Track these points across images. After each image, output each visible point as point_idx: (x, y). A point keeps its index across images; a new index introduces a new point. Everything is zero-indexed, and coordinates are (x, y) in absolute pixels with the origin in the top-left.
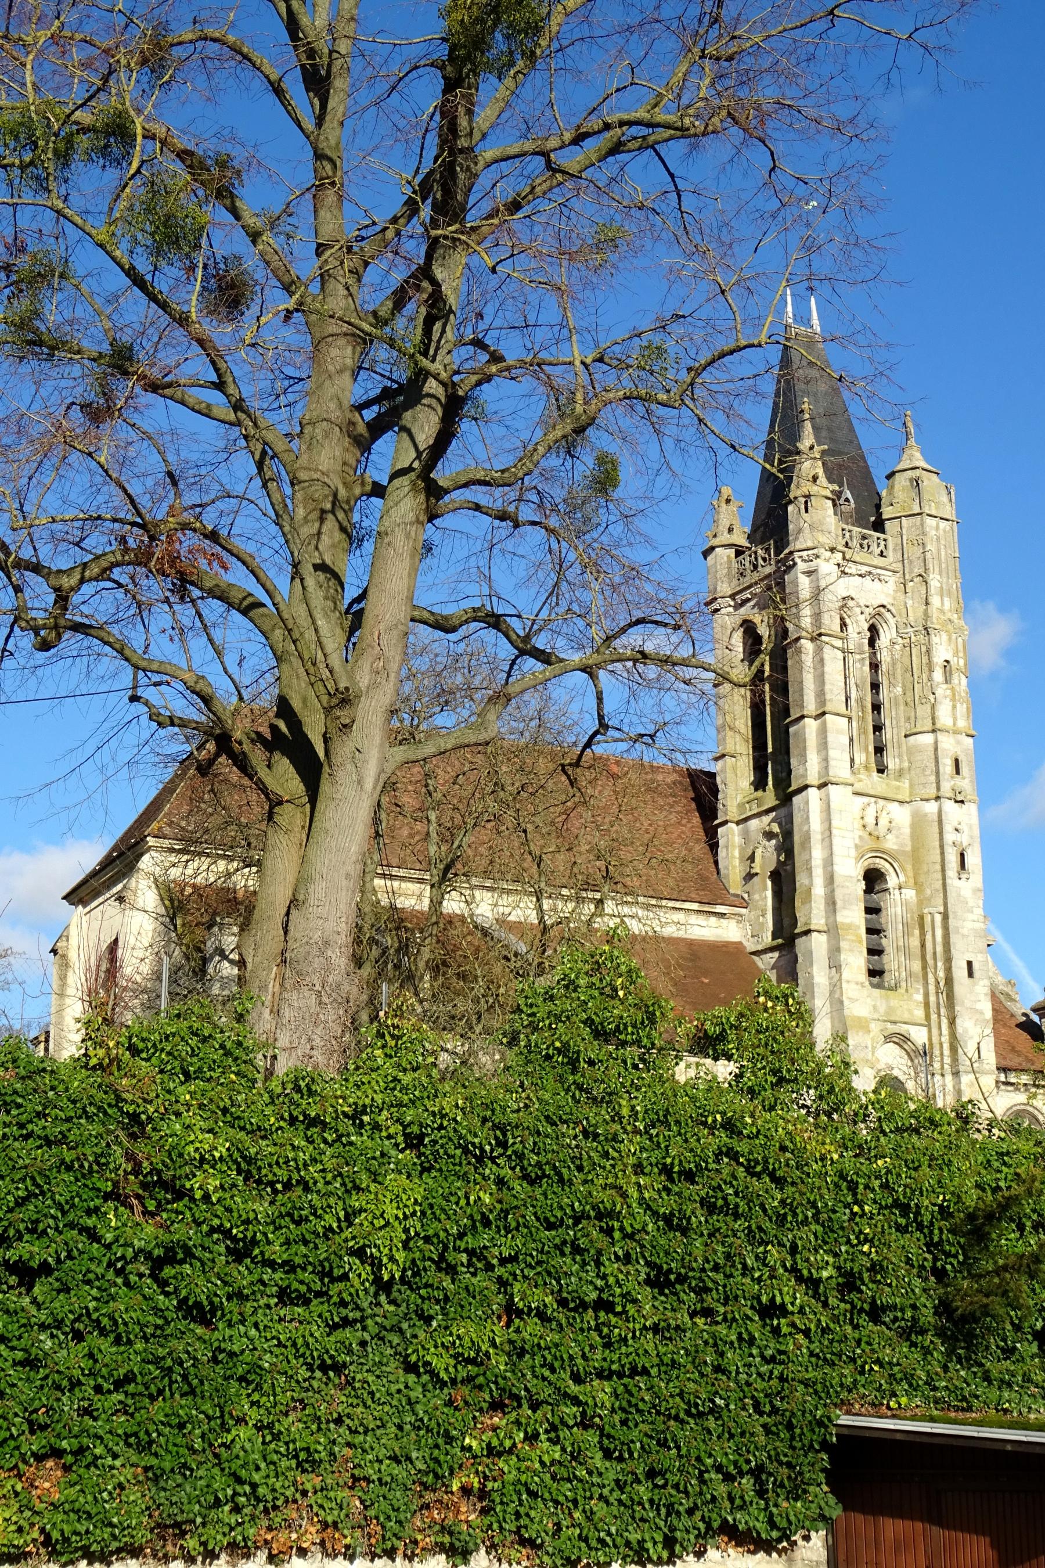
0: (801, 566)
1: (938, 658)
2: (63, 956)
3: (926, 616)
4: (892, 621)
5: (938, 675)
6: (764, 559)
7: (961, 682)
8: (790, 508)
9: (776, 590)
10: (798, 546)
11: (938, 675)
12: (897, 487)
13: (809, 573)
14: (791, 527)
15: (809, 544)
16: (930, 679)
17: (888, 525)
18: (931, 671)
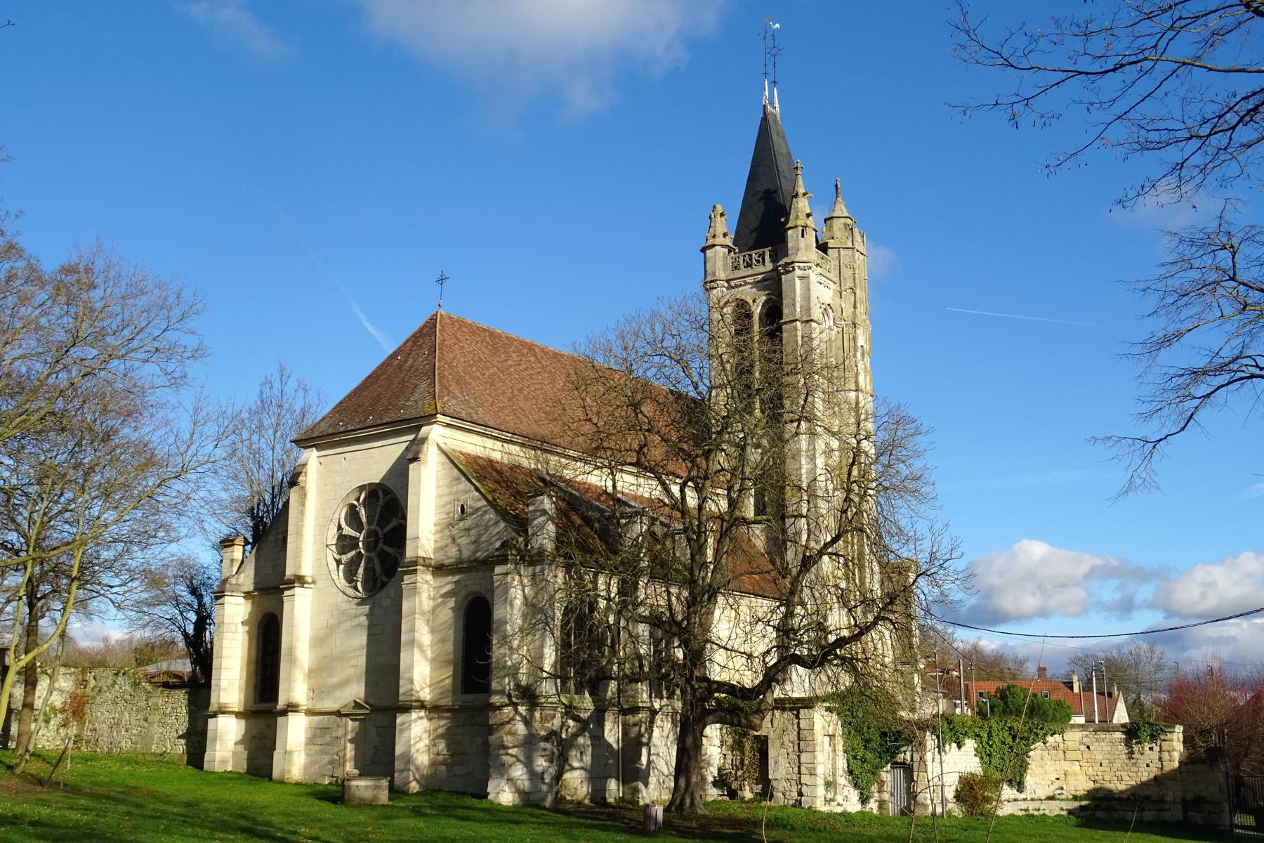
0: (798, 272)
1: (859, 345)
2: (303, 488)
3: (854, 314)
4: (831, 315)
5: (859, 355)
6: (758, 261)
7: (867, 359)
8: (790, 232)
9: (773, 285)
10: (797, 259)
11: (859, 355)
12: (835, 227)
13: (801, 278)
14: (790, 245)
15: (805, 259)
16: (855, 356)
17: (830, 251)
18: (856, 351)
